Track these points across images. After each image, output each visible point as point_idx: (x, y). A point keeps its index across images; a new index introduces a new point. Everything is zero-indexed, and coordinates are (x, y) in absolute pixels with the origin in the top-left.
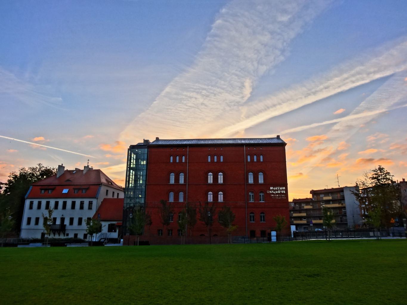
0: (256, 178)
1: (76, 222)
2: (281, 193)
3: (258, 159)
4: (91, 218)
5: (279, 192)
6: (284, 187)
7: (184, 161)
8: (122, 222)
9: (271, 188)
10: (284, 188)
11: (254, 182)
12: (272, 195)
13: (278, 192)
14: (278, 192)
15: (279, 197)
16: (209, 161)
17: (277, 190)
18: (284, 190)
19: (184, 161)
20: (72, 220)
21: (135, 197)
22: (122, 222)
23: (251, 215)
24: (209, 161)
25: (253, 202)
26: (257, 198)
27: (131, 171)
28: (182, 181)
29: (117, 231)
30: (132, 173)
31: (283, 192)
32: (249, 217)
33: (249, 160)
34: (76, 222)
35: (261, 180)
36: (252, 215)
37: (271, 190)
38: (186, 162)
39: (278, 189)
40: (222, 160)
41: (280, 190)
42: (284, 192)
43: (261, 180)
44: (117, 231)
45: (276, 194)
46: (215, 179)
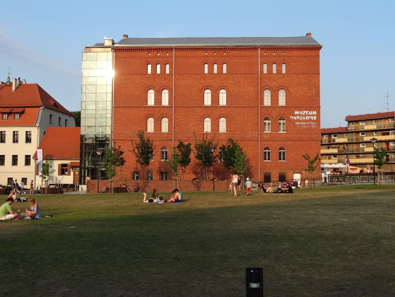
0: (275, 98)
2: (310, 120)
3: (279, 71)
5: (307, 118)
6: (315, 112)
7: (168, 72)
9: (297, 113)
10: (315, 113)
11: (271, 104)
12: (297, 123)
13: (306, 118)
14: (306, 118)
15: (306, 125)
16: (206, 71)
17: (306, 115)
18: (315, 115)
19: (168, 72)
21: (107, 127)
23: (265, 151)
24: (206, 71)
25: (270, 132)
26: (276, 127)
28: (165, 102)
31: (312, 119)
32: (263, 154)
33: (265, 71)
35: (282, 101)
36: (267, 151)
37: (297, 115)
39: (307, 114)
40: (225, 71)
41: (309, 115)
42: (315, 118)
44: (72, 173)
45: (303, 121)
46: (215, 98)
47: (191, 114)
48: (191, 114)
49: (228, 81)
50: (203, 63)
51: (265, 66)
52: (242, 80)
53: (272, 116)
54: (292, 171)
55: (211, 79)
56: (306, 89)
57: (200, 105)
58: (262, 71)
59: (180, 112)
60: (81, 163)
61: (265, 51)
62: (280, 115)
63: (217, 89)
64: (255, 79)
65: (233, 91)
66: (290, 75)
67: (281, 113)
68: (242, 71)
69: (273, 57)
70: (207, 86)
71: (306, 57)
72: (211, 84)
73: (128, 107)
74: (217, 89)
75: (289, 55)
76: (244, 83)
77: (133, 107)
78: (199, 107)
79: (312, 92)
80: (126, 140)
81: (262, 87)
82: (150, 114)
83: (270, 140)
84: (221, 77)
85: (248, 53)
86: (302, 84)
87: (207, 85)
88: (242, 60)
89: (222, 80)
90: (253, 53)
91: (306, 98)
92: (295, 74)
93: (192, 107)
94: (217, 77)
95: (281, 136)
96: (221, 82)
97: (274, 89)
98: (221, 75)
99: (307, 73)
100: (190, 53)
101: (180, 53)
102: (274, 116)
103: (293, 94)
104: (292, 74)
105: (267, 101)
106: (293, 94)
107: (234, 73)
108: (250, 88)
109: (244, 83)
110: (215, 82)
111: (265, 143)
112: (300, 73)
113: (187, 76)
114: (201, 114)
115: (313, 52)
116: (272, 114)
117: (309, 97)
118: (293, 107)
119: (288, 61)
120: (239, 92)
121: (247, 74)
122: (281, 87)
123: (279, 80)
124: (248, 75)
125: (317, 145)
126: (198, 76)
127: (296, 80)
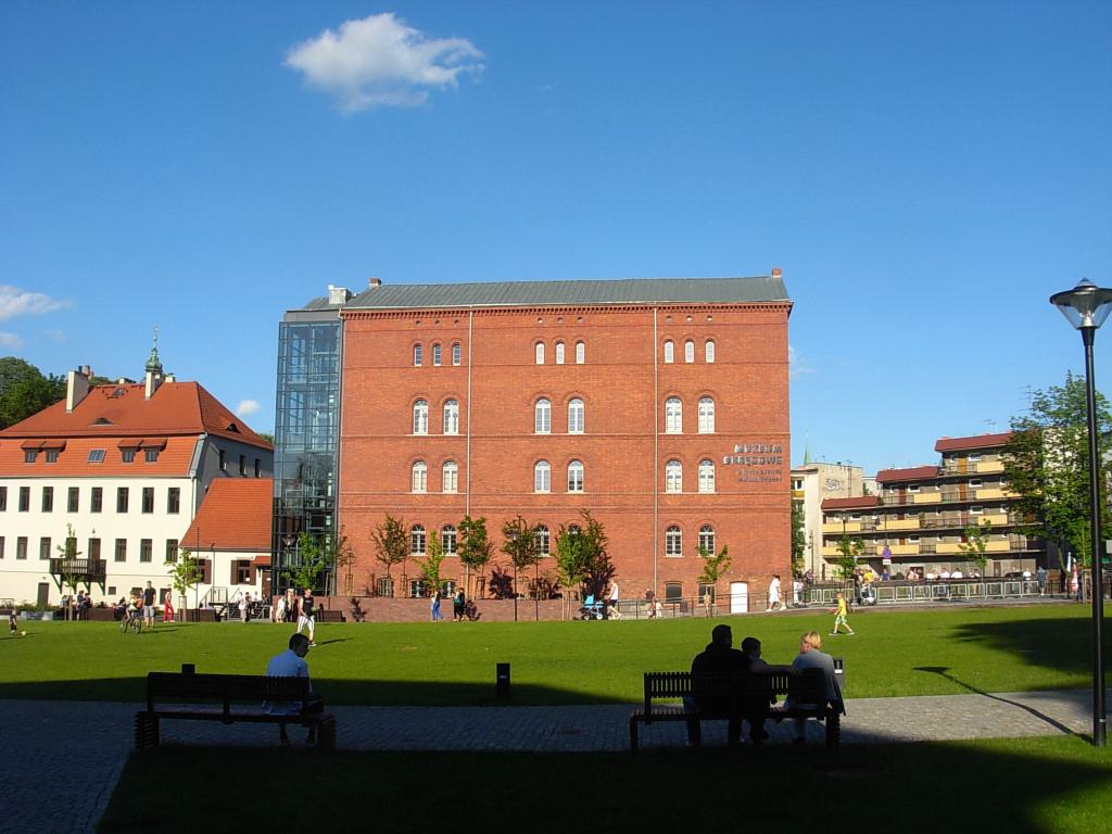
0: (690, 419)
1: (134, 550)
4: (176, 541)
8: (270, 555)
16: (540, 361)
20: (121, 546)
22: (270, 555)
24: (540, 361)
27: (294, 395)
29: (259, 580)
30: (298, 401)
33: (669, 359)
34: (134, 550)
35: (707, 425)
36: (674, 533)
38: (464, 367)
40: (580, 360)
43: (707, 425)
46: (560, 419)
50: (534, 342)
51: (669, 347)
53: (683, 456)
55: (549, 377)
58: (662, 357)
59: (483, 448)
60: (274, 558)
62: (701, 454)
63: (564, 398)
65: (598, 402)
67: (705, 450)
70: (542, 392)
73: (371, 438)
74: (564, 398)
75: (721, 321)
76: (623, 384)
77: (383, 438)
78: (523, 436)
80: (366, 509)
82: (418, 455)
83: (680, 511)
85: (631, 318)
86: (749, 385)
90: (643, 317)
93: (508, 437)
95: (704, 501)
97: (689, 396)
100: (504, 321)
101: (482, 320)
102: (687, 457)
103: (730, 408)
104: (727, 363)
105: (674, 426)
106: (730, 408)
107: (600, 362)
108: (636, 396)
109: (623, 384)
111: (668, 516)
113: (498, 369)
114: (530, 452)
115: (774, 316)
116: (683, 453)
117: (765, 413)
118: (729, 436)
119: (719, 336)
122: (706, 396)
124: (631, 368)
125: (783, 520)
126: (521, 369)
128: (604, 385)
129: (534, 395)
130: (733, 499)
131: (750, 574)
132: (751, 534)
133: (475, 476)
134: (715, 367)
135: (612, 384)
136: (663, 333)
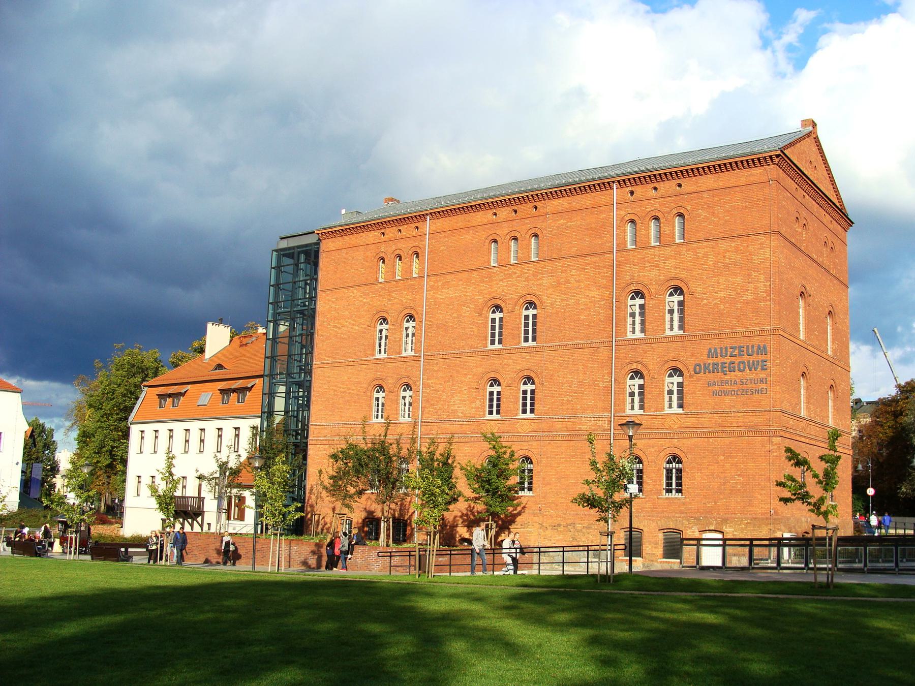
47: (458, 372)
48: (458, 372)
49: (541, 279)
52: (573, 272)
54: (695, 524)
56: (739, 279)
57: (477, 348)
61: (630, 189)
64: (605, 267)
66: (695, 245)
68: (574, 249)
69: (652, 201)
70: (494, 298)
71: (738, 189)
72: (503, 291)
79: (756, 288)
81: (623, 285)
84: (526, 271)
86: (726, 266)
87: (494, 294)
88: (573, 222)
89: (527, 280)
91: (739, 305)
92: (708, 240)
94: (515, 273)
96: (526, 283)
98: (527, 265)
99: (741, 232)
107: (554, 256)
109: (579, 281)
110: (513, 285)
112: (722, 235)
119: (689, 208)
120: (565, 306)
121: (586, 256)
123: (665, 263)
127: (712, 258)
128: (559, 284)
129: (486, 303)
130: (704, 420)
131: (725, 521)
132: (728, 465)
133: (427, 401)
134: (683, 249)
135: (568, 282)
136: (623, 213)
